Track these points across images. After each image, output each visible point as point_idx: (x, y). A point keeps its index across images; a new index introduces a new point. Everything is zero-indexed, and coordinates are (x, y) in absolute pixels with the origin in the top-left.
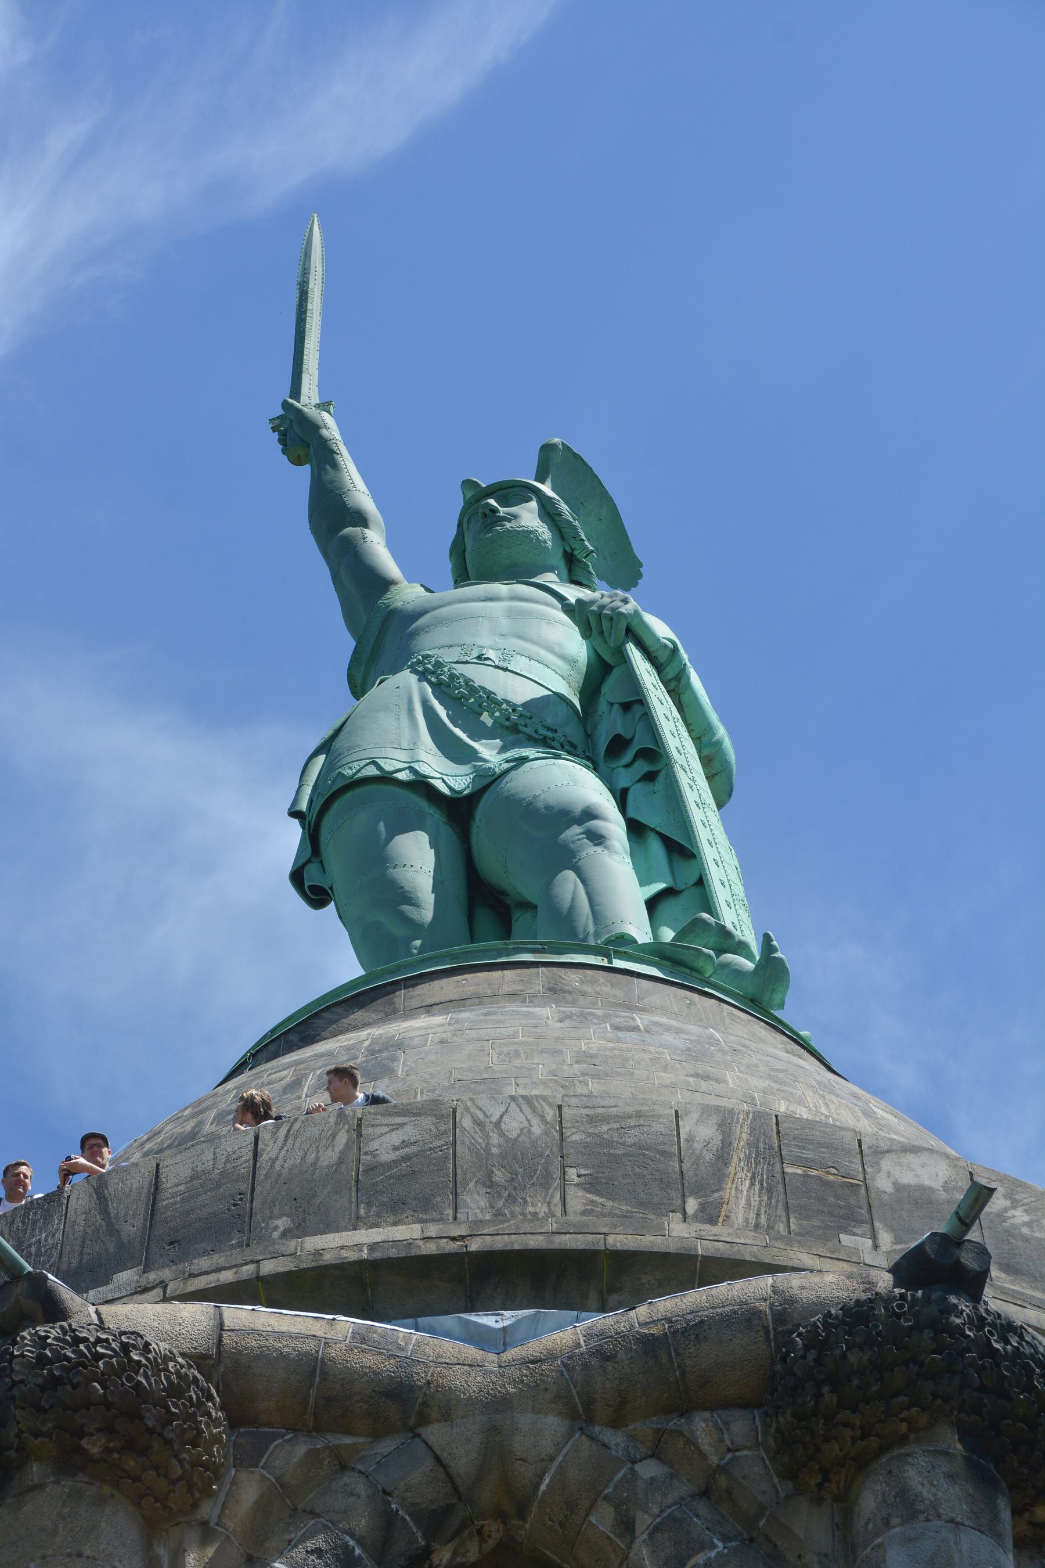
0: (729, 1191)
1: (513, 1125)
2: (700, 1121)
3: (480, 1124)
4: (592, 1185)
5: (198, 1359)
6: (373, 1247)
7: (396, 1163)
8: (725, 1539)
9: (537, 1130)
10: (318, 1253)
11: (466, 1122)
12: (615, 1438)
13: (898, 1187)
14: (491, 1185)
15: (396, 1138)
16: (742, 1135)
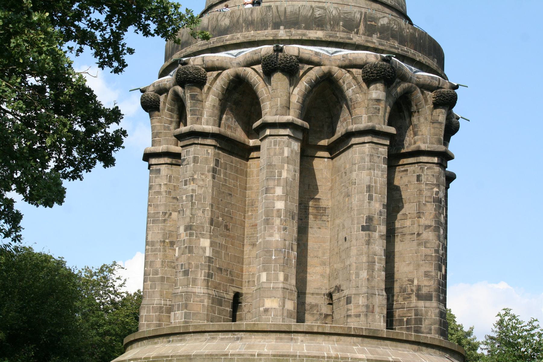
0: (360, 28)
1: (334, 12)
2: (358, 14)
3: (330, 12)
4: (343, 26)
5: (297, 57)
6: (317, 38)
7: (318, 17)
8: (355, 86)
9: (337, 14)
10: (310, 38)
11: (328, 11)
12: (344, 70)
13: (381, 25)
14: (330, 24)
15: (318, 13)
16: (363, 17)
